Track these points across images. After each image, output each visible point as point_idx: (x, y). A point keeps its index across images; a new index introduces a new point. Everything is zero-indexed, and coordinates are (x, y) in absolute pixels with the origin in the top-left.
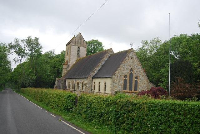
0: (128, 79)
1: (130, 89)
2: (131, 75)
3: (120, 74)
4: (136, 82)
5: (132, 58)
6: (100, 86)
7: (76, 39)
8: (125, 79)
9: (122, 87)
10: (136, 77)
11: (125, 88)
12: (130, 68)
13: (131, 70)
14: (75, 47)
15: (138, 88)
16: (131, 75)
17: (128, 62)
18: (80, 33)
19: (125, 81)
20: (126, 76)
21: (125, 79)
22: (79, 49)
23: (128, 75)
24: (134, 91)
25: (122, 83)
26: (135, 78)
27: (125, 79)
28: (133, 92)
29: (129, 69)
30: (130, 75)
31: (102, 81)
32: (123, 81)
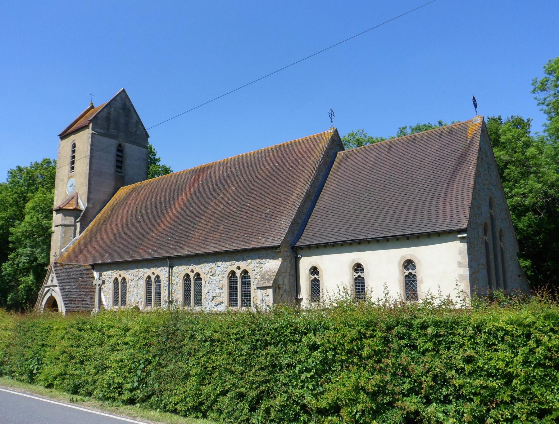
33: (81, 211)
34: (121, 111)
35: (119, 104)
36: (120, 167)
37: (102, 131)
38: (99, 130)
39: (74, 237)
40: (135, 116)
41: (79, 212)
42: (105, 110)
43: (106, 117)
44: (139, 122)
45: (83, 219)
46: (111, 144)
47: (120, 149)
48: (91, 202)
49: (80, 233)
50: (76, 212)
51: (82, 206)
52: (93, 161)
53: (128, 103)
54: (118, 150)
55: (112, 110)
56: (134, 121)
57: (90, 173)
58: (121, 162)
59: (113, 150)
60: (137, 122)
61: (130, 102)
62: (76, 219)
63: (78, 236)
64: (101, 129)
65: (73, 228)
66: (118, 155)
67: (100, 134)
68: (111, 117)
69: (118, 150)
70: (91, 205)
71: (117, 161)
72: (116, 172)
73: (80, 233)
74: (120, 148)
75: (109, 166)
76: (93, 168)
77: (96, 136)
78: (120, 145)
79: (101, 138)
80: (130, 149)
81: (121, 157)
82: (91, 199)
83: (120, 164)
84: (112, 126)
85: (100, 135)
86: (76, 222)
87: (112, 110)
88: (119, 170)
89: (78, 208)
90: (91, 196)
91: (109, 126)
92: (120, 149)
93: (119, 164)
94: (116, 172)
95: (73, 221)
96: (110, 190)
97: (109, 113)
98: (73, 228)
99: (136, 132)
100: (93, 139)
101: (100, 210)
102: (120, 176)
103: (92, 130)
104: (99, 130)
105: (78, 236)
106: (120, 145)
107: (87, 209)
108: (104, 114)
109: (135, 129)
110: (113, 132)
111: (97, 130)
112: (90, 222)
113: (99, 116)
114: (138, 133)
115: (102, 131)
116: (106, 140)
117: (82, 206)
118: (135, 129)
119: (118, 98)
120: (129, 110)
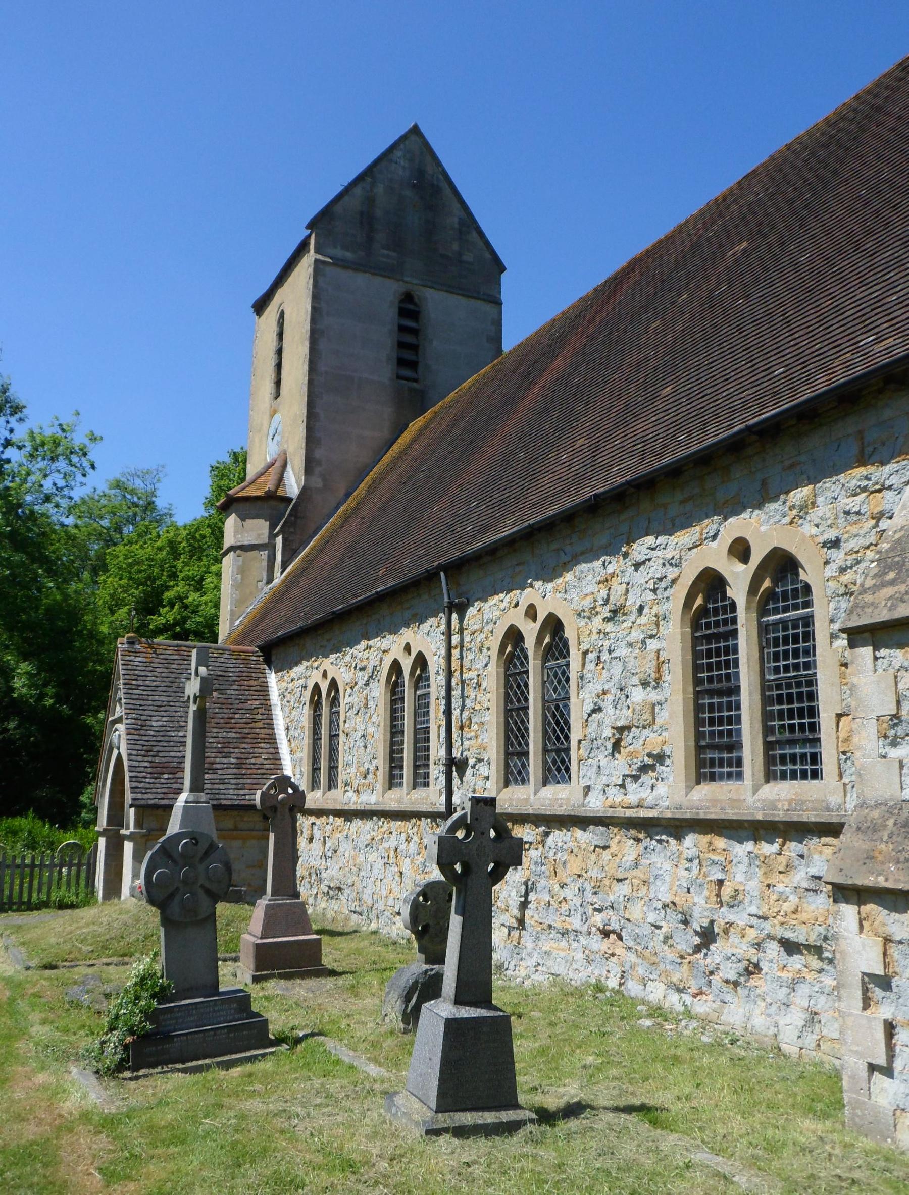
34: (408, 193)
36: (413, 365)
37: (349, 255)
38: (339, 252)
39: (270, 581)
40: (457, 205)
41: (282, 506)
42: (358, 191)
45: (294, 524)
46: (383, 293)
47: (409, 309)
48: (318, 470)
50: (270, 504)
51: (293, 485)
52: (322, 345)
55: (380, 189)
57: (310, 383)
58: (414, 348)
59: (389, 313)
61: (438, 163)
62: (272, 527)
63: (279, 578)
64: (345, 248)
65: (264, 554)
67: (339, 263)
68: (379, 213)
69: (403, 313)
70: (317, 482)
71: (401, 345)
72: (399, 377)
73: (284, 568)
74: (411, 307)
75: (375, 361)
76: (322, 368)
77: (328, 270)
78: (408, 297)
81: (415, 332)
82: (319, 463)
83: (409, 353)
84: (381, 237)
85: (345, 268)
87: (380, 189)
89: (280, 493)
90: (318, 454)
91: (370, 239)
92: (409, 309)
93: (408, 355)
94: (399, 377)
96: (386, 433)
97: (370, 200)
98: (264, 554)
101: (348, 495)
103: (317, 251)
104: (339, 252)
106: (408, 297)
107: (304, 491)
108: (354, 202)
112: (315, 533)
113: (338, 208)
115: (349, 255)
116: (360, 280)
117: (293, 485)
118: (455, 247)
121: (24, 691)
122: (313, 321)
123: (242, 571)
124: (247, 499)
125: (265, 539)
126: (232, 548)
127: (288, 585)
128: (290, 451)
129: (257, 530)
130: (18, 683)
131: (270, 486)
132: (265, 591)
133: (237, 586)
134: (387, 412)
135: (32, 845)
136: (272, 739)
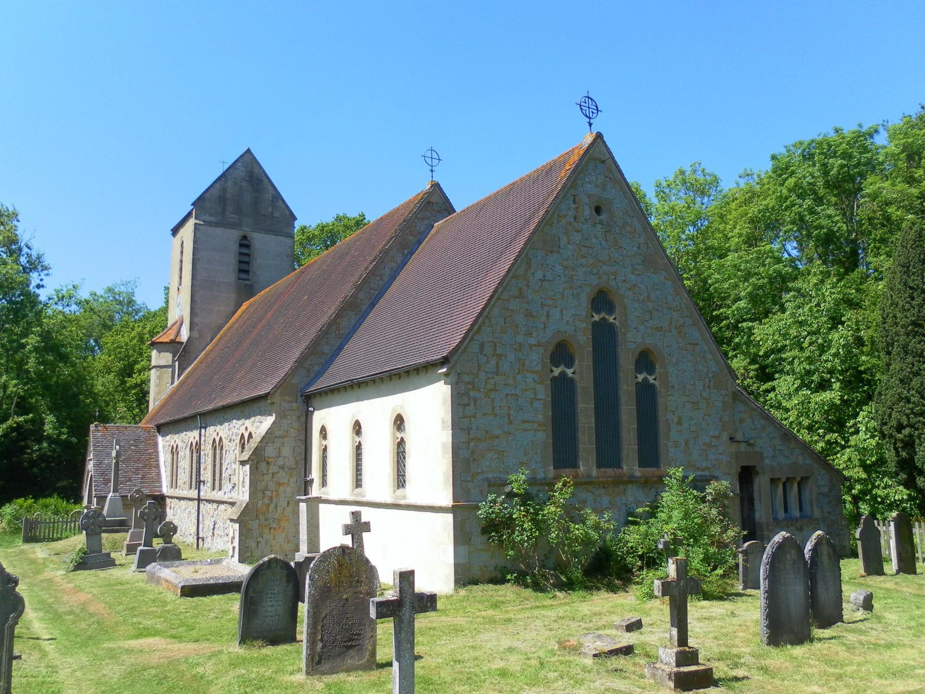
0: (581, 372)
1: (608, 455)
2: (605, 338)
3: (520, 338)
4: (647, 397)
5: (598, 210)
6: (359, 447)
7: (224, 190)
8: (563, 374)
9: (543, 437)
10: (645, 361)
11: (564, 454)
12: (594, 280)
13: (602, 301)
14: (219, 231)
15: (662, 441)
16: (605, 338)
17: (577, 237)
18: (248, 151)
19: (562, 391)
20: (561, 353)
21: (563, 374)
22: (248, 246)
23: (583, 342)
24: (638, 472)
25: (538, 409)
26: (638, 370)
27: (557, 372)
28: (632, 480)
29: (585, 299)
30: (594, 335)
31: (375, 411)
32: (544, 393)
33: (182, 343)
34: (244, 184)
35: (241, 172)
37: (213, 219)
38: (207, 218)
42: (218, 185)
43: (220, 197)
44: (277, 197)
45: (184, 356)
47: (245, 244)
49: (179, 376)
51: (184, 335)
52: (198, 266)
53: (256, 170)
54: (241, 245)
55: (230, 183)
56: (269, 196)
59: (234, 247)
60: (274, 197)
62: (174, 357)
63: (176, 383)
64: (211, 215)
66: (241, 254)
67: (208, 224)
68: (229, 196)
70: (196, 334)
73: (179, 376)
74: (245, 242)
75: (227, 273)
76: (199, 277)
77: (202, 227)
78: (245, 237)
79: (210, 230)
80: (261, 241)
82: (197, 325)
83: (244, 267)
86: (174, 361)
87: (230, 183)
88: (243, 276)
90: (196, 320)
91: (224, 211)
92: (245, 244)
93: (244, 267)
95: (171, 359)
97: (224, 190)
99: (272, 214)
100: (198, 233)
101: (212, 340)
102: (246, 285)
105: (176, 383)
106: (245, 237)
109: (270, 210)
110: (232, 217)
111: (204, 218)
112: (195, 359)
113: (207, 195)
114: (277, 214)
115: (213, 219)
119: (239, 164)
120: (260, 181)
121: (51, 431)
122: (193, 254)
123: (159, 378)
124: (162, 343)
125: (170, 363)
126: (154, 367)
127: (181, 384)
128: (185, 317)
129: (166, 358)
130: (47, 427)
131: (172, 337)
132: (170, 388)
133: (157, 386)
134: (233, 296)
135: (56, 513)
136: (158, 466)
